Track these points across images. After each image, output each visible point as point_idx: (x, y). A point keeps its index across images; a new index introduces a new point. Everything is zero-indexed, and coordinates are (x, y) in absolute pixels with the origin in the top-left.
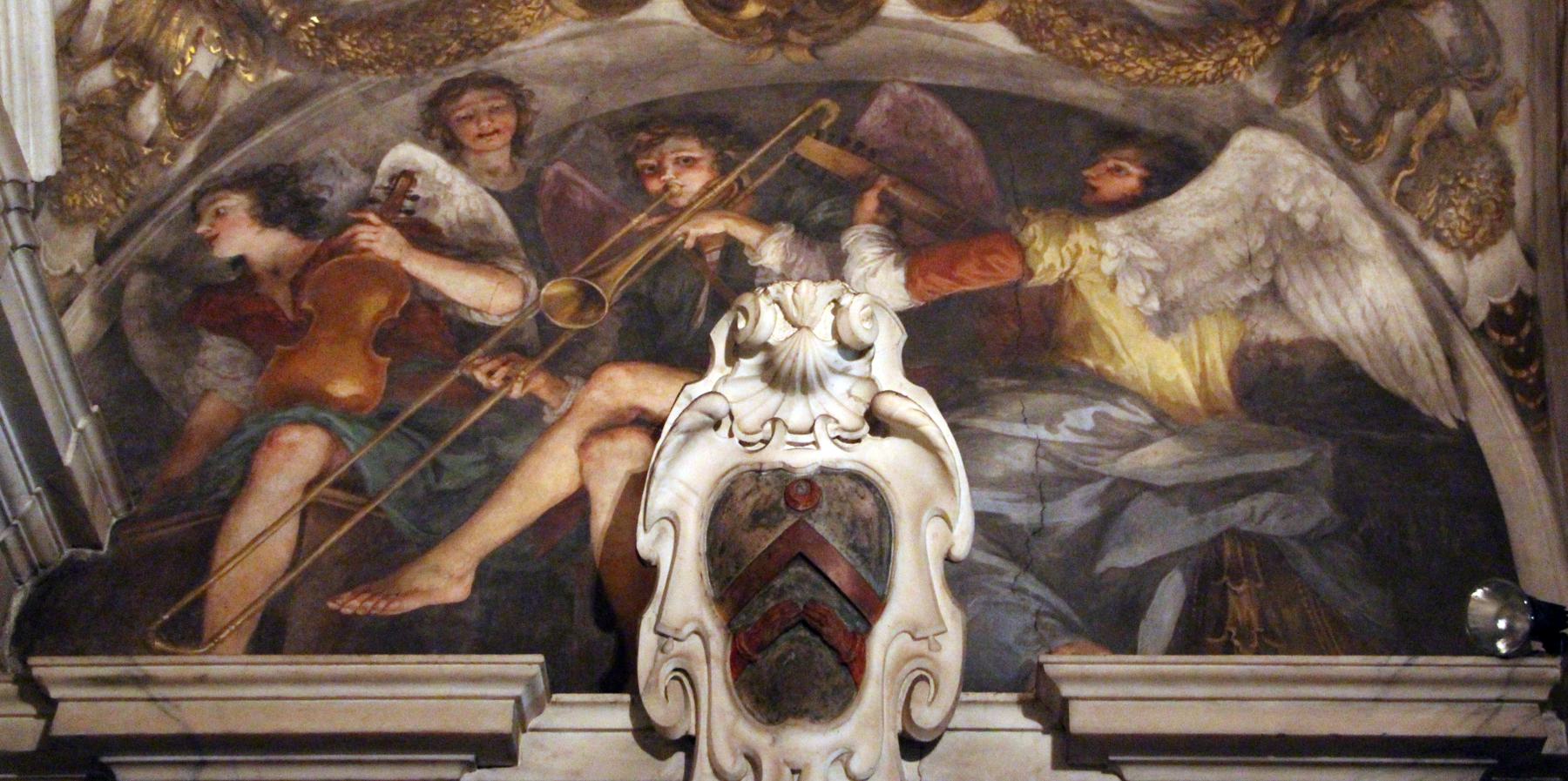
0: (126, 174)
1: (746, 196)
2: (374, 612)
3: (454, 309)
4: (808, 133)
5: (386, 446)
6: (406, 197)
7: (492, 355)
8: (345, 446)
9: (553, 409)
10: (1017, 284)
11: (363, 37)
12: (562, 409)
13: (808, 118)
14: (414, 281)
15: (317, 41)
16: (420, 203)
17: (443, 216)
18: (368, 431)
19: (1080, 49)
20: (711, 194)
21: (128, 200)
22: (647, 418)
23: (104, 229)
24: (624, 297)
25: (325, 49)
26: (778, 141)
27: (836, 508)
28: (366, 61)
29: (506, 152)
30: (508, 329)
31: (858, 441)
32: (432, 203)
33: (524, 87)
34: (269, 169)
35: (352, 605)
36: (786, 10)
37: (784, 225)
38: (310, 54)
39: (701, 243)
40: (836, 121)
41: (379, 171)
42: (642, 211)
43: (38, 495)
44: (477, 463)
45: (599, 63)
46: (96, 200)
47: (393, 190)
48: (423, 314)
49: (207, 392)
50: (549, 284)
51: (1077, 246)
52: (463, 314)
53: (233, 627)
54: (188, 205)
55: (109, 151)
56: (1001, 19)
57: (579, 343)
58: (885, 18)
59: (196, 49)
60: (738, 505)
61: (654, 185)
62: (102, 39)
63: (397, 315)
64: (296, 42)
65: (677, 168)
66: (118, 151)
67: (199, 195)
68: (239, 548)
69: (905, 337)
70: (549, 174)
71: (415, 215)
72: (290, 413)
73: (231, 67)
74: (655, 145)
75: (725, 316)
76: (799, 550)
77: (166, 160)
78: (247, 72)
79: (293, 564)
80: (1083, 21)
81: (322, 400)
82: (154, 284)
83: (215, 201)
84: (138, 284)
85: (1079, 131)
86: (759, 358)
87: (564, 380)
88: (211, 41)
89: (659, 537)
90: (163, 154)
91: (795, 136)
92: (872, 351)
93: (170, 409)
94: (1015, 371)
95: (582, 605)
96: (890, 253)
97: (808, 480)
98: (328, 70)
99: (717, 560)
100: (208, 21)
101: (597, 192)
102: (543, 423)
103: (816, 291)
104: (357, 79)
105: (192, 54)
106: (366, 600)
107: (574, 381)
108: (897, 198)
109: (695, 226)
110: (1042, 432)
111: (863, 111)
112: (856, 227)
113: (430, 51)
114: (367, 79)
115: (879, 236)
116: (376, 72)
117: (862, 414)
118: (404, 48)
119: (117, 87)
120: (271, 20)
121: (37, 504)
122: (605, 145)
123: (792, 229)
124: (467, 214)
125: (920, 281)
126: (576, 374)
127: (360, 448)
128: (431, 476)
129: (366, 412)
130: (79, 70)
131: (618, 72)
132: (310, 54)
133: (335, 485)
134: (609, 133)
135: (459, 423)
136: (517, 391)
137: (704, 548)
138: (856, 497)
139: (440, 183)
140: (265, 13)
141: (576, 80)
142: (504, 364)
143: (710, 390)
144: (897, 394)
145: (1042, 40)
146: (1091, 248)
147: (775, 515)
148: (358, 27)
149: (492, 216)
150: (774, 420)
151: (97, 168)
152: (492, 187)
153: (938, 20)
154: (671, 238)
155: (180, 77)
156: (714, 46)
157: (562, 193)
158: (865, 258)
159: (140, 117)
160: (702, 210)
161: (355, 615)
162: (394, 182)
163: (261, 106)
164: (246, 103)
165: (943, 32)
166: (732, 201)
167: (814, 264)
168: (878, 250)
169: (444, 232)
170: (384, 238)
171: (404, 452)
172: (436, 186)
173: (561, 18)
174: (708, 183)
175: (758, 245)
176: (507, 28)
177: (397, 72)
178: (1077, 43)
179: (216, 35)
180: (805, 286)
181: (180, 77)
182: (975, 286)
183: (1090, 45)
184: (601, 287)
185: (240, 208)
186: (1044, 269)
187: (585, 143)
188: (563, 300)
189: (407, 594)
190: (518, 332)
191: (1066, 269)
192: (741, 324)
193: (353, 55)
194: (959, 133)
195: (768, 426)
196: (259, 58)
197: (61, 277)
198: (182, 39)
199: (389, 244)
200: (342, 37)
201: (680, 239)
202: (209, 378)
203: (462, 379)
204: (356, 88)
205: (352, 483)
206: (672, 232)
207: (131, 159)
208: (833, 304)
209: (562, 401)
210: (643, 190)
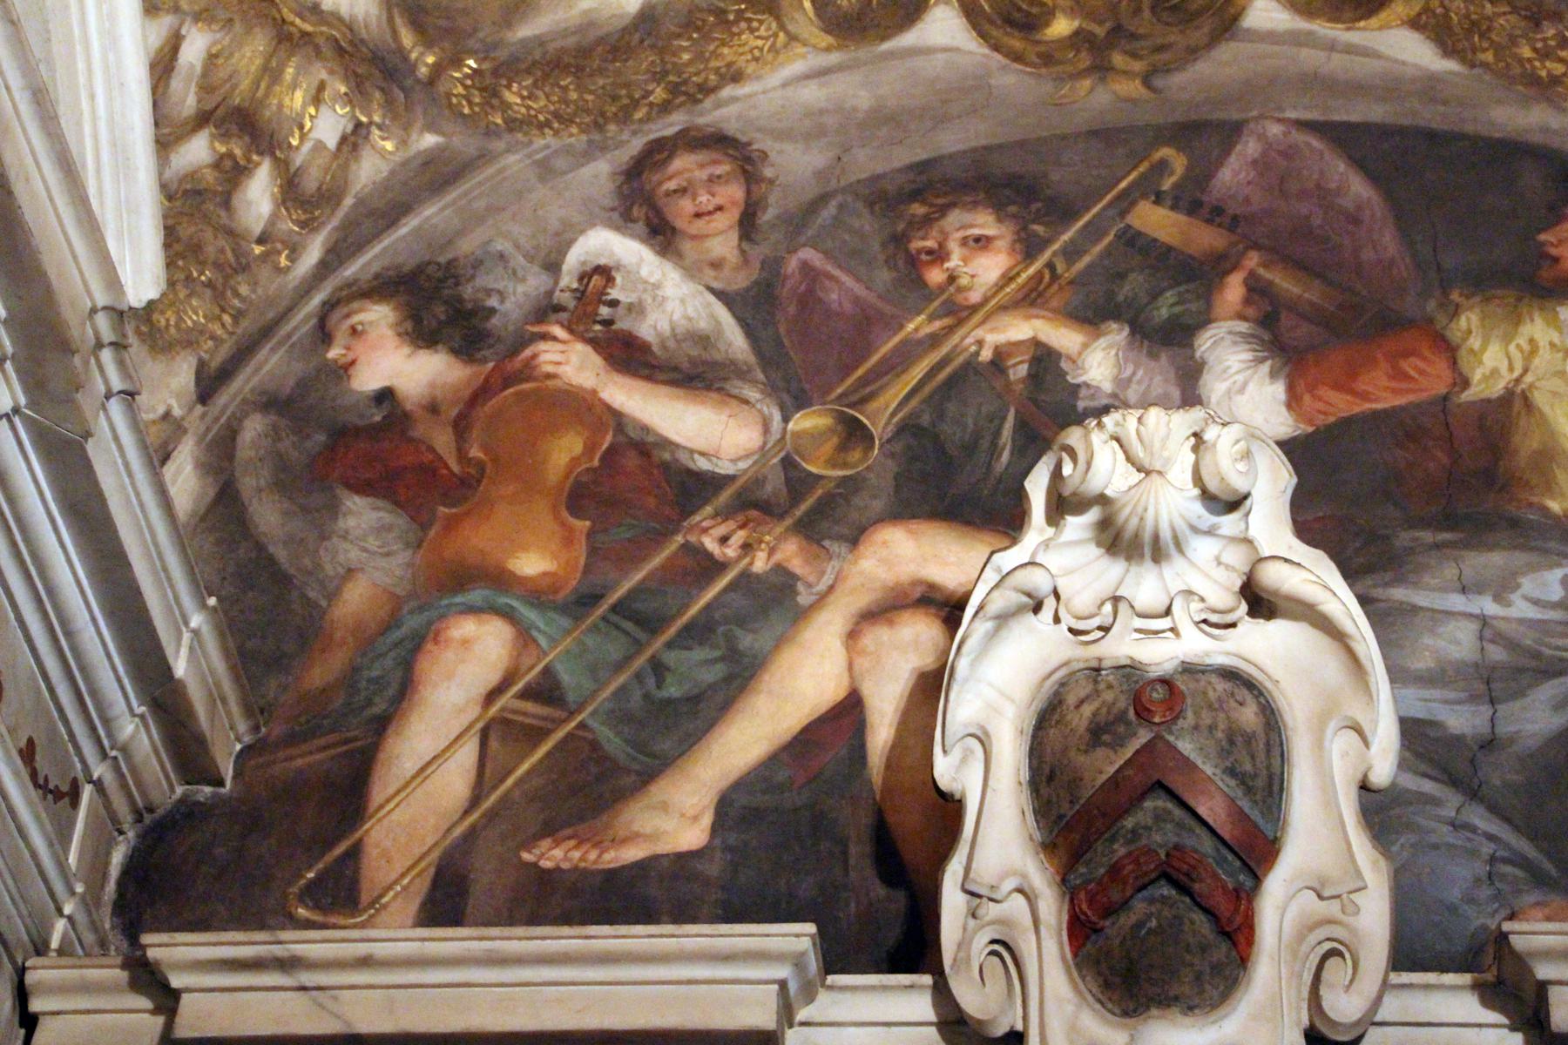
0: (232, 282)
1: (1061, 288)
2: (583, 865)
3: (673, 453)
4: (1144, 196)
5: (590, 641)
6: (600, 302)
7: (724, 515)
8: (535, 641)
9: (810, 586)
10: (1445, 398)
11: (535, 84)
12: (822, 587)
13: (1143, 177)
14: (618, 418)
16: (621, 310)
17: (651, 327)
18: (565, 622)
19: (1530, 60)
20: (1013, 286)
22: (938, 596)
23: (206, 356)
24: (902, 429)
25: (486, 103)
26: (1104, 209)
27: (1207, 718)
28: (541, 118)
29: (734, 236)
30: (745, 478)
31: (1233, 625)
32: (637, 309)
33: (755, 147)
34: (420, 270)
35: (554, 855)
36: (1108, 25)
37: (1114, 326)
38: (466, 111)
39: (1001, 356)
40: (1186, 177)
41: (565, 267)
42: (919, 314)
43: (142, 717)
44: (712, 662)
45: (855, 109)
46: (195, 318)
47: (583, 292)
48: (631, 461)
49: (350, 572)
50: (798, 415)
51: (1531, 341)
52: (683, 457)
53: (398, 888)
54: (314, 321)
55: (210, 250)
56: (1414, 24)
57: (840, 494)
58: (1248, 30)
59: (317, 110)
60: (1069, 718)
61: (935, 276)
62: (194, 104)
63: (596, 463)
64: (449, 95)
65: (965, 251)
66: (222, 251)
67: (329, 306)
68: (402, 782)
69: (1295, 480)
70: (792, 264)
71: (614, 327)
72: (459, 599)
73: (364, 132)
74: (937, 219)
75: (1044, 459)
76: (1156, 777)
77: (283, 261)
78: (383, 139)
79: (475, 801)
80: (1536, 21)
81: (501, 579)
82: (275, 427)
83: (348, 316)
84: (254, 427)
85: (1531, 180)
86: (1093, 515)
87: (823, 547)
88: (337, 97)
89: (964, 760)
90: (279, 253)
91: (1126, 202)
92: (1248, 502)
93: (304, 596)
94: (1449, 521)
95: (859, 852)
96: (1262, 361)
97: (1165, 682)
98: (490, 132)
99: (1044, 791)
100: (331, 72)
101: (859, 290)
102: (797, 604)
103: (1169, 421)
104: (531, 142)
105: (311, 117)
106: (570, 850)
107: (835, 547)
108: (1270, 283)
109: (992, 330)
110: (1488, 606)
111: (1220, 162)
112: (1214, 325)
113: (626, 101)
114: (545, 142)
115: (1247, 337)
116: (556, 133)
117: (1237, 588)
118: (590, 97)
119: (217, 165)
120: (413, 68)
121: (142, 729)
122: (865, 220)
123: (1126, 331)
124: (683, 322)
125: (1307, 398)
126: (840, 538)
127: (554, 642)
128: (651, 682)
129: (561, 596)
131: (885, 120)
132: (466, 111)
133: (524, 695)
134: (871, 204)
135: (687, 606)
136: (760, 564)
137: (1025, 775)
138: (1233, 704)
139: (646, 282)
140: (405, 59)
141: (825, 135)
142: (741, 527)
143: (1026, 561)
144: (1286, 560)
145: (1474, 50)
146: (1552, 345)
147: (1121, 729)
148: (528, 72)
149: (718, 323)
150: (1116, 600)
151: (195, 274)
152: (716, 285)
153: (1323, 29)
154: (959, 350)
155: (297, 148)
156: (1011, 80)
157: (810, 291)
158: (1229, 367)
159: (249, 203)
160: (1003, 308)
161: (558, 869)
162: (586, 280)
163: (405, 184)
164: (387, 179)
165: (1331, 47)
166: (1040, 295)
167: (1158, 379)
168: (1248, 356)
169: (655, 349)
170: (574, 359)
171: (614, 649)
172: (640, 287)
173: (801, 50)
174: (1011, 269)
175: (1080, 354)
176: (729, 65)
177: (583, 131)
178: (1526, 52)
179: (343, 89)
180: (1154, 414)
181: (297, 148)
182: (1386, 401)
183: (1545, 54)
184: (868, 418)
185: (383, 322)
186: (1484, 374)
187: (837, 221)
188: (816, 436)
189: (625, 841)
190: (759, 482)
191: (1516, 374)
192: (1067, 469)
193: (523, 110)
194: (1358, 188)
195: (1108, 607)
196: (400, 119)
197: (154, 422)
198: (299, 97)
199: (581, 368)
200: (509, 87)
201: (973, 348)
202: (353, 555)
203: (686, 547)
204: (529, 156)
205: (546, 691)
206: (963, 339)
207: (237, 258)
208: (1193, 440)
209: (823, 573)
210: (921, 283)
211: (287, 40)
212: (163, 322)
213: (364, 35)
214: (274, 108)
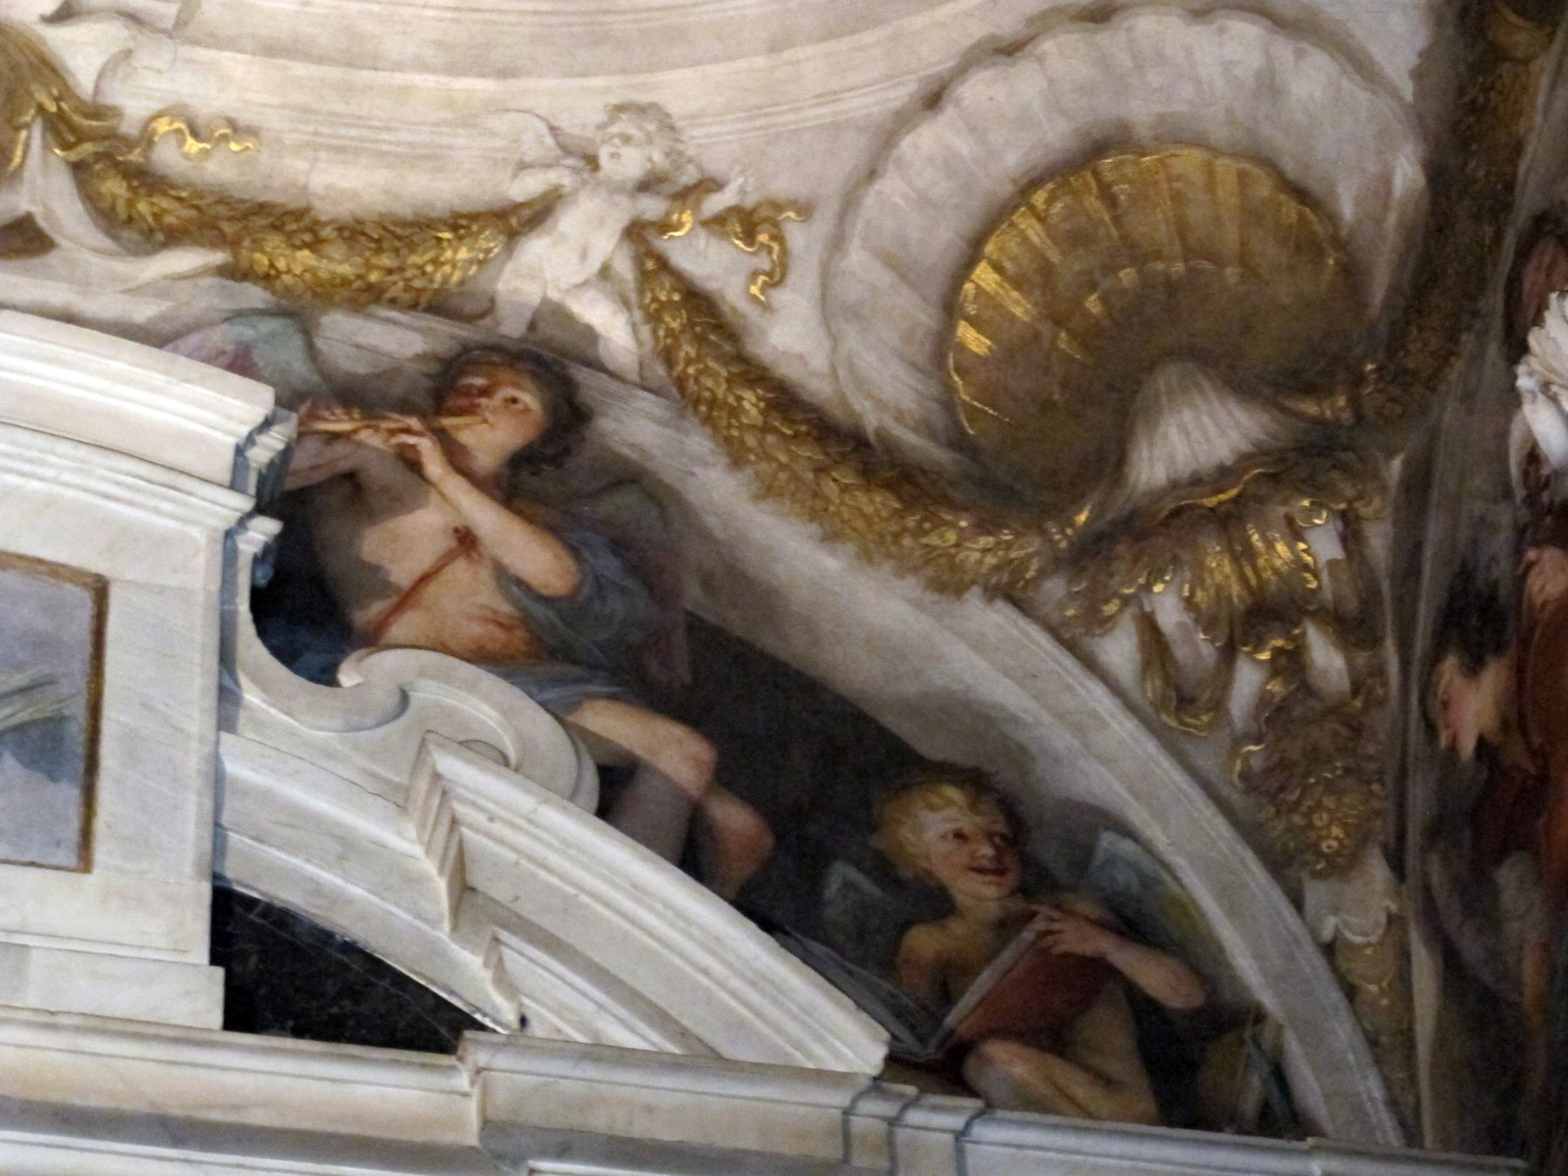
15: (1390, 388)
21: (1381, 782)
46: (1354, 812)
54: (1422, 724)
55: (1326, 744)
66: (1335, 734)
88: (1310, 513)
100: (1285, 502)
105: (1304, 551)
119: (1274, 669)
130: (1218, 706)
151: (1329, 776)
155: (1320, 587)
179: (1306, 503)
181: (1320, 587)
198: (1281, 548)
200: (1407, 354)
211: (1228, 521)
212: (1335, 844)
213: (1280, 445)
214: (1273, 578)
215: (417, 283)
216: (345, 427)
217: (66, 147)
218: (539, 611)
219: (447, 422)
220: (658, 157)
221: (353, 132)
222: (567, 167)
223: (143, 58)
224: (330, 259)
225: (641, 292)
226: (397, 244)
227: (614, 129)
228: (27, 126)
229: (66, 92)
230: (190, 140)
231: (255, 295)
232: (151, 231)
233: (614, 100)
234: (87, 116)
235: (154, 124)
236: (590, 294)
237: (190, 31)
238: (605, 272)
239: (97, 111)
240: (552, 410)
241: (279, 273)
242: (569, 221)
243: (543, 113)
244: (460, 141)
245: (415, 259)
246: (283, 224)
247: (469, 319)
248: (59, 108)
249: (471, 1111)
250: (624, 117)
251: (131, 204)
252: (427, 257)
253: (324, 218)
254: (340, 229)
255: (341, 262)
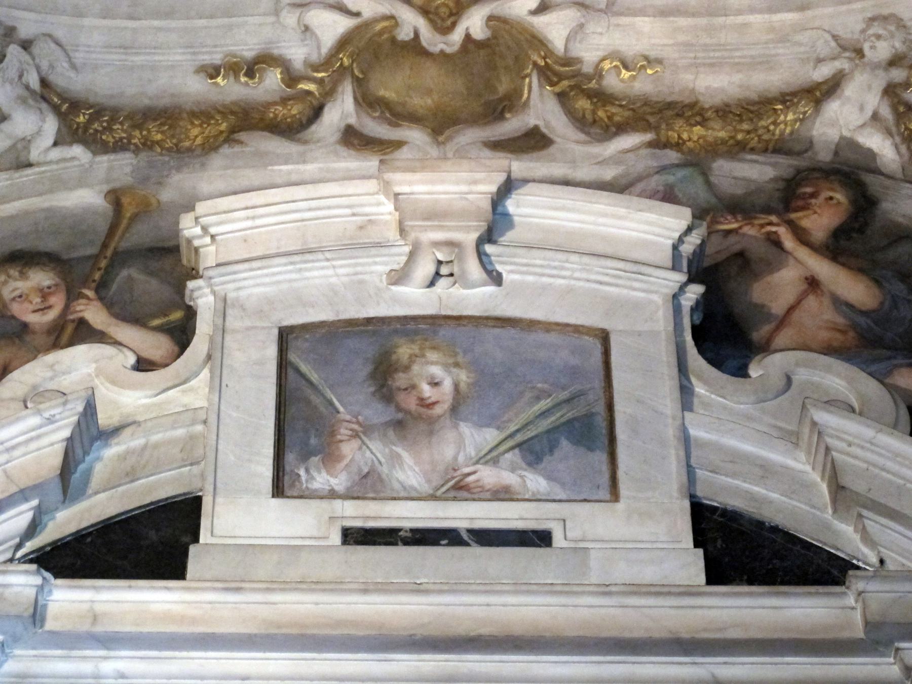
215: (766, 137)
216: (735, 226)
217: (552, 84)
218: (862, 321)
219: (793, 216)
220: (898, 45)
221: (717, 54)
222: (845, 58)
223: (591, 28)
224: (713, 129)
225: (898, 124)
226: (751, 115)
227: (871, 32)
228: (529, 75)
229: (549, 53)
230: (624, 71)
231: (672, 156)
232: (607, 127)
233: (869, 15)
234: (564, 65)
235: (602, 65)
236: (868, 130)
237: (615, 9)
238: (875, 117)
239: (568, 61)
240: (853, 202)
241: (684, 142)
242: (850, 90)
243: (827, 28)
244: (781, 51)
245: (763, 123)
246: (684, 113)
247: (799, 154)
248: (546, 62)
249: (858, 617)
250: (876, 24)
251: (594, 112)
252: (769, 121)
253: (707, 106)
254: (717, 111)
255: (719, 131)
